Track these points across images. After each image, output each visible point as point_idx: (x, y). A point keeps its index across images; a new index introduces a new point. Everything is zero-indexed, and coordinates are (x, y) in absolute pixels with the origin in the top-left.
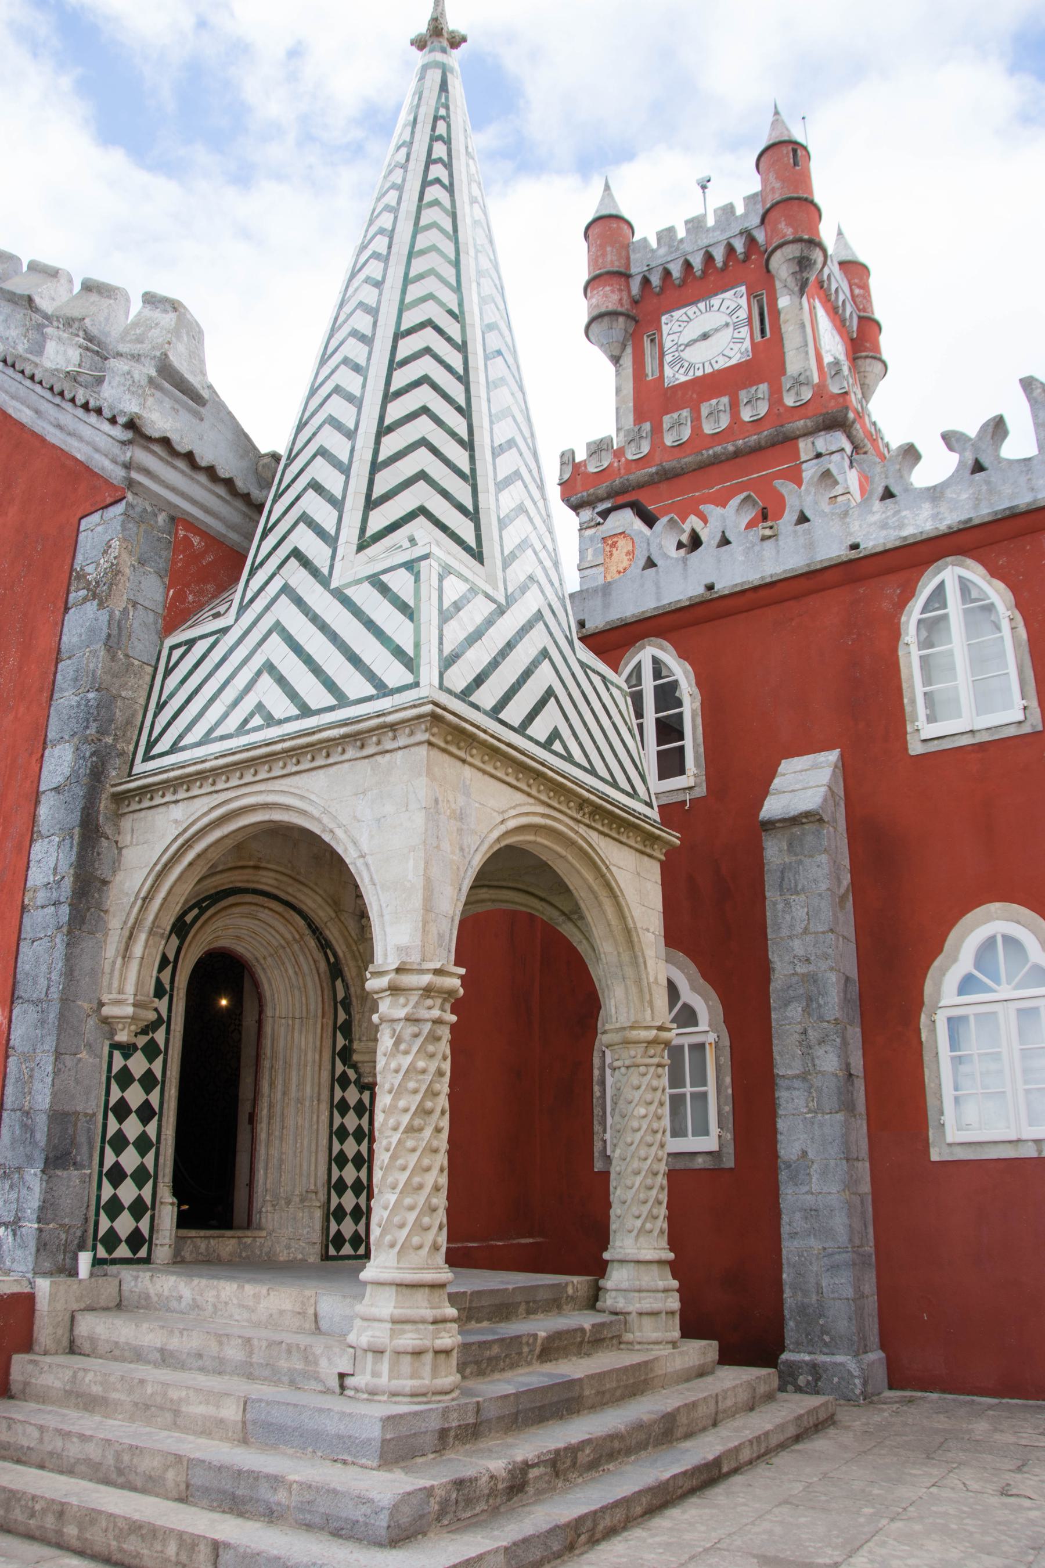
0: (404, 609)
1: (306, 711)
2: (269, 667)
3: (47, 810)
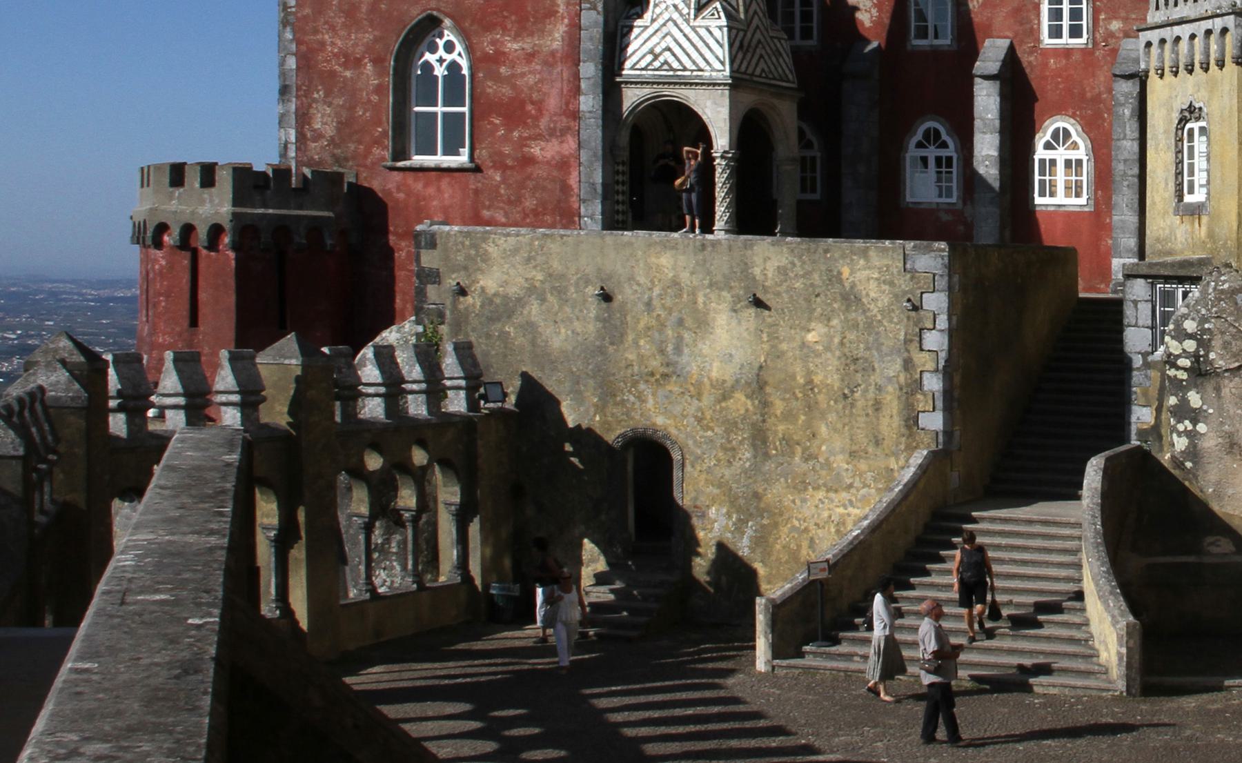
0: (718, 42)
1: (685, 69)
2: (668, 49)
3: (583, 85)
